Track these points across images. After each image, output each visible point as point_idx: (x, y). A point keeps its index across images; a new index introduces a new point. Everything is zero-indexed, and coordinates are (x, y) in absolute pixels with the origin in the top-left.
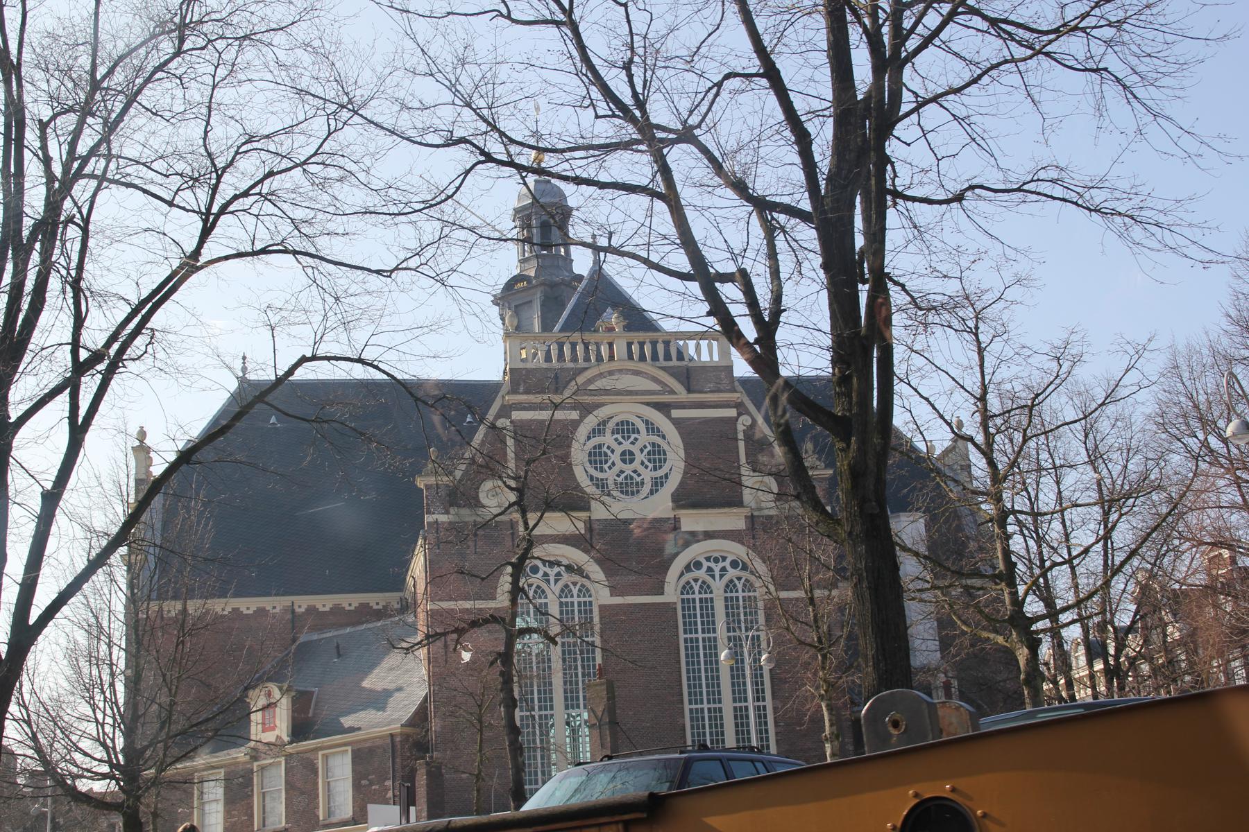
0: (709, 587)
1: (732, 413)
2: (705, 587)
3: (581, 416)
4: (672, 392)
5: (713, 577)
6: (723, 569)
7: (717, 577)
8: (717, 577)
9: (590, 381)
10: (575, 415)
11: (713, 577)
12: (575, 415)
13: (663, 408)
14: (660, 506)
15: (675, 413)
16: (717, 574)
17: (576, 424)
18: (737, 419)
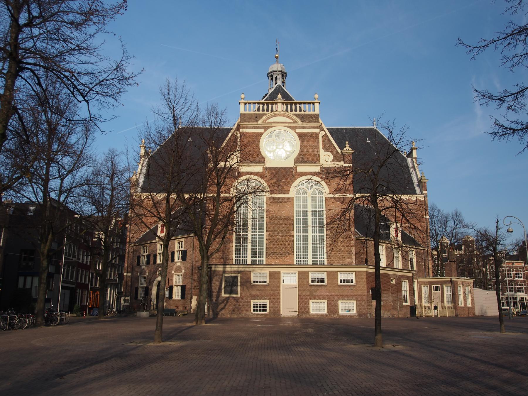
0: (306, 192)
1: (317, 130)
2: (305, 193)
3: (264, 130)
4: (296, 122)
5: (308, 188)
6: (312, 186)
7: (309, 189)
8: (309, 189)
9: (268, 119)
10: (262, 130)
11: (308, 188)
12: (262, 130)
13: (293, 128)
14: (290, 163)
15: (297, 130)
16: (309, 188)
17: (261, 134)
18: (320, 132)
